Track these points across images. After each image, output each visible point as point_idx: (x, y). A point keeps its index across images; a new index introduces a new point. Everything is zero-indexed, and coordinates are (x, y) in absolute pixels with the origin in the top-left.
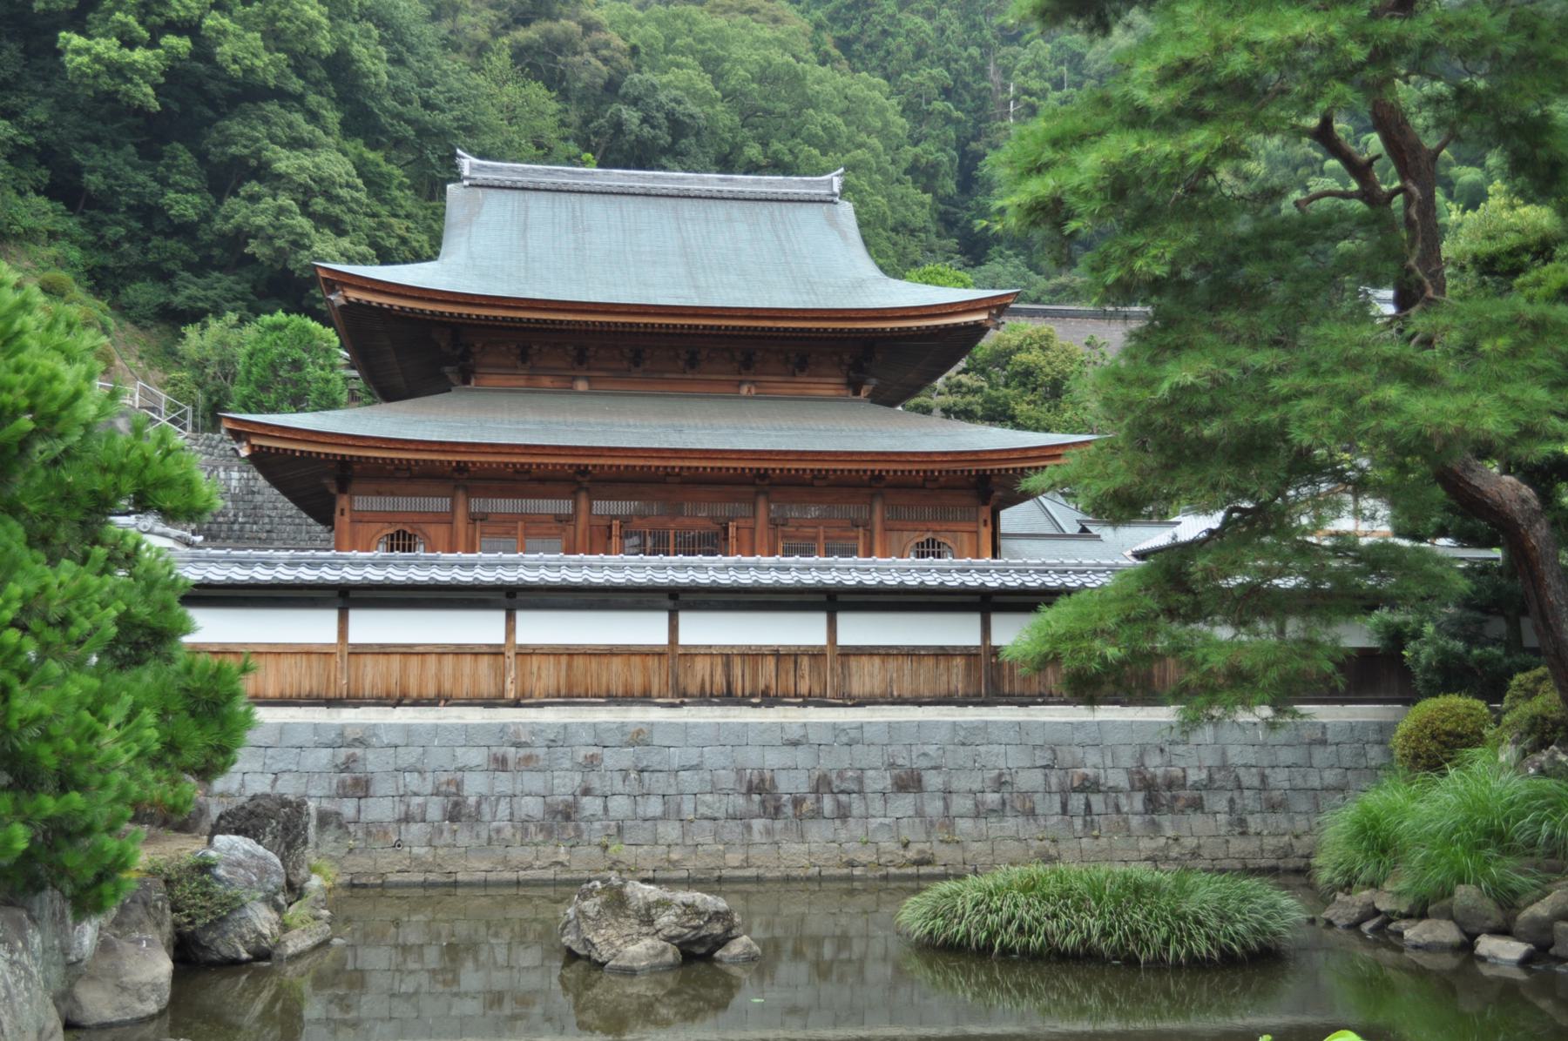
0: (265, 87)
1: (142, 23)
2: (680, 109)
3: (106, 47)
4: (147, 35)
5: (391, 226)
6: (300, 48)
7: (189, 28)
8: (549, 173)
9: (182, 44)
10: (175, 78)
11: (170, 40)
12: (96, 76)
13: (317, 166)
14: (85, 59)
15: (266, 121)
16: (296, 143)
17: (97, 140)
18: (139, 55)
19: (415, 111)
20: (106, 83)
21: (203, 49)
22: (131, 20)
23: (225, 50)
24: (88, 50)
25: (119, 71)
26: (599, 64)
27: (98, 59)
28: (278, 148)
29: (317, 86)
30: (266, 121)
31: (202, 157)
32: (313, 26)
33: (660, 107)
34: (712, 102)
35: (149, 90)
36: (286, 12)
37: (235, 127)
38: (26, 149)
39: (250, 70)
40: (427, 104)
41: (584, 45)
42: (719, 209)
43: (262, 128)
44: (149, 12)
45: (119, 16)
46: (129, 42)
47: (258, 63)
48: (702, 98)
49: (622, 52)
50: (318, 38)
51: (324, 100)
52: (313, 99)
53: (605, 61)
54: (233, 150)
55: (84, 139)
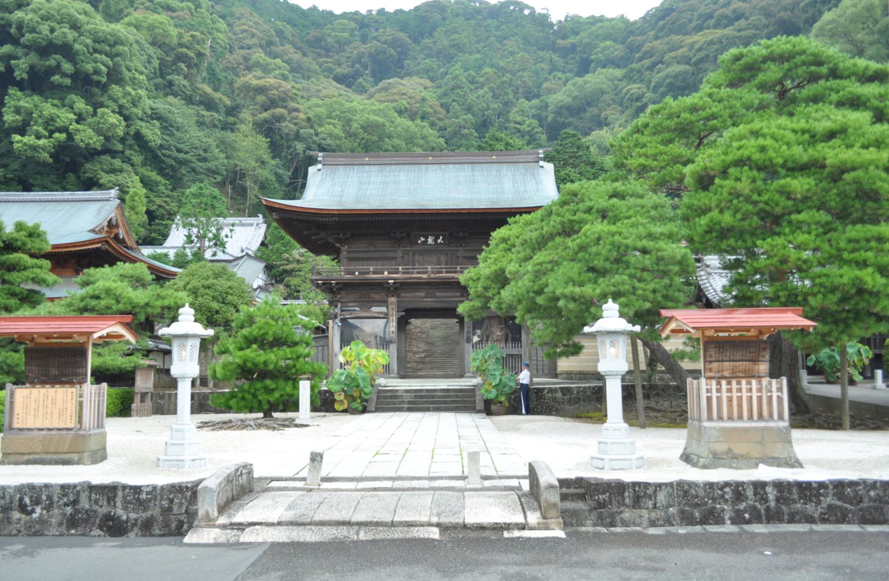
0: (95, 149)
1: (46, 129)
2: (324, 142)
3: (30, 139)
4: (47, 134)
5: (154, 202)
6: (110, 134)
7: (64, 129)
8: (6, 195)
9: (62, 136)
10: (59, 151)
11: (57, 135)
12: (26, 150)
13: (117, 180)
14: (20, 145)
15: (101, 163)
16: (113, 171)
17: (41, 174)
18: (41, 142)
19: (175, 154)
20: (29, 153)
21: (70, 137)
22: (40, 129)
23: (77, 137)
24: (21, 141)
25: (35, 148)
26: (292, 126)
27: (25, 144)
28: (103, 174)
29: (131, 147)
30: (101, 163)
31: (79, 177)
32: (114, 126)
33: (315, 142)
34: (340, 139)
35: (46, 155)
36: (102, 121)
37: (88, 166)
38: (11, 179)
39: (89, 144)
40: (179, 151)
41: (288, 118)
42: (67, 206)
43: (99, 166)
44: (49, 125)
45: (35, 127)
46: (38, 137)
47: (91, 141)
48: (337, 137)
49: (303, 120)
50: (117, 130)
51: (133, 152)
52: (128, 152)
53: (295, 124)
54: (87, 175)
55: (36, 174)
